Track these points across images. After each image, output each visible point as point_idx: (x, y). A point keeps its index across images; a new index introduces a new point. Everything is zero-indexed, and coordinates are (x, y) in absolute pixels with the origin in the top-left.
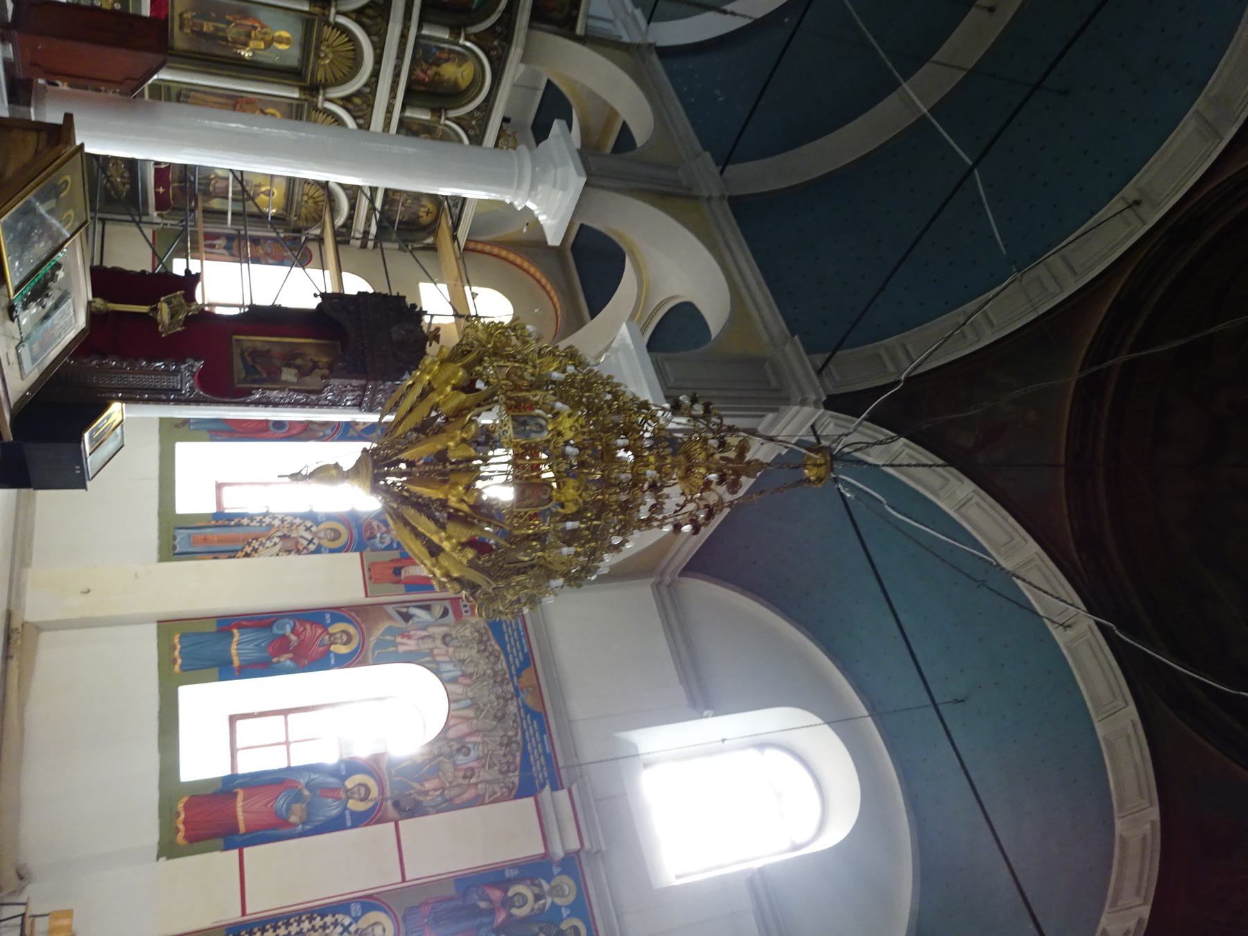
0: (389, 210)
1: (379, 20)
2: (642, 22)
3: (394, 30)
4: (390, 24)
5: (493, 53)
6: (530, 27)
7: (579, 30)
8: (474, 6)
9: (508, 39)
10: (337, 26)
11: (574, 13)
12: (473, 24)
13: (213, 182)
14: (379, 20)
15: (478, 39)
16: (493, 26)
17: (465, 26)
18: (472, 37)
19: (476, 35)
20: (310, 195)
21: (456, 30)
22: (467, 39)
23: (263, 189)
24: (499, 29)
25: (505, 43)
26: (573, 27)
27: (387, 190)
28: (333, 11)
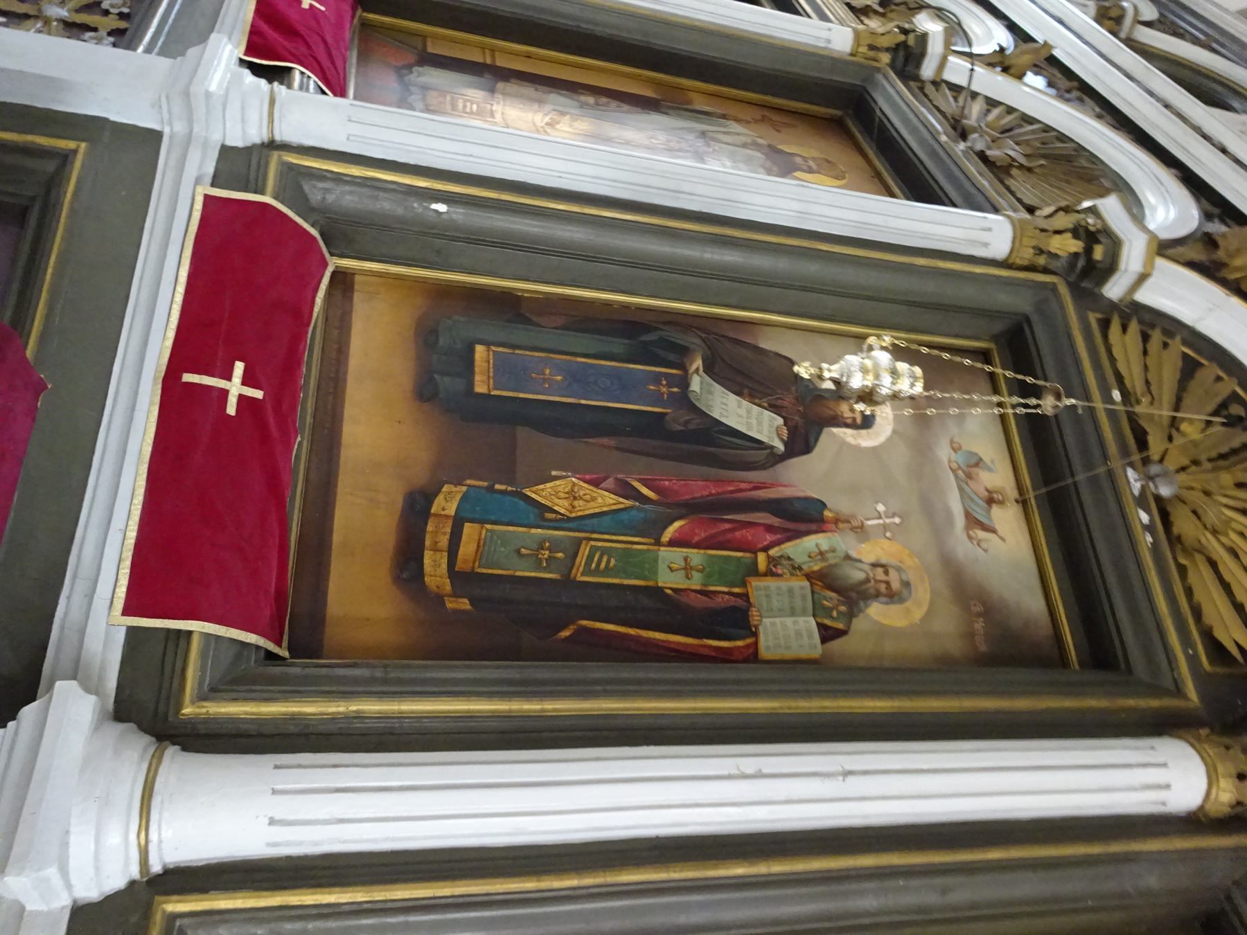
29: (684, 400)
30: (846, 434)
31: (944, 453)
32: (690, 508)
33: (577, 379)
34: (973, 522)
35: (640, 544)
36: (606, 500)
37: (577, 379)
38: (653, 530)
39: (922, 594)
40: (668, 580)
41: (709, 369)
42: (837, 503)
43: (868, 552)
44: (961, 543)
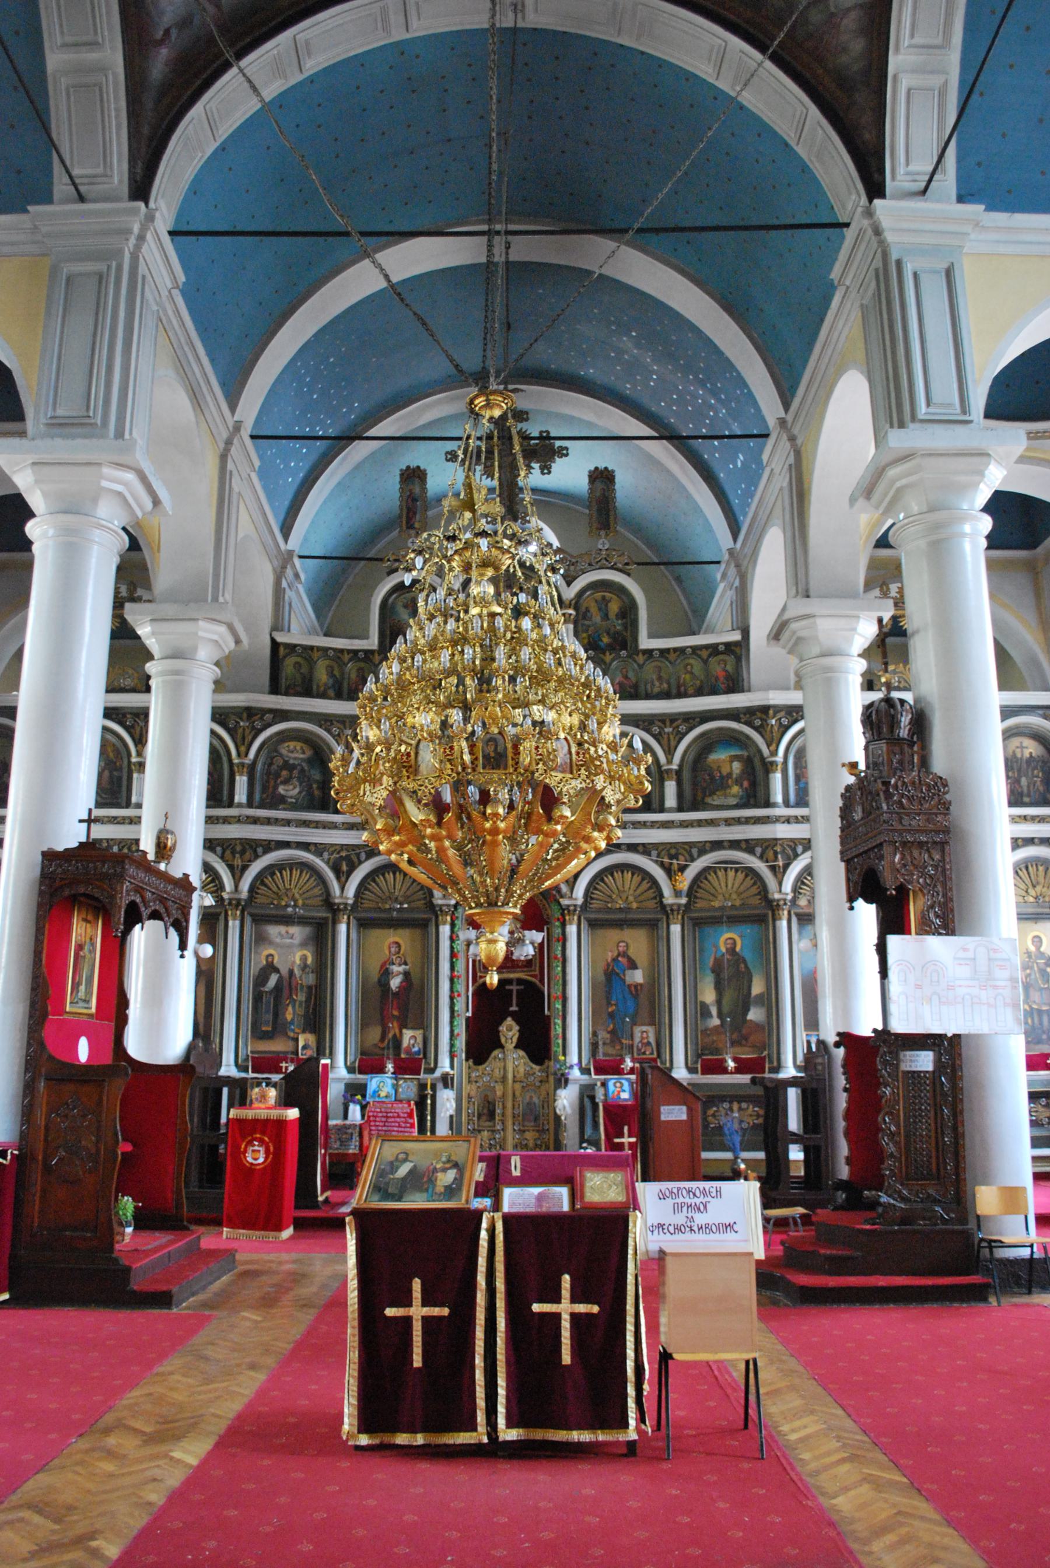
0: (1029, 795)
1: (778, 849)
2: (723, 566)
3: (782, 831)
4: (779, 836)
5: (785, 721)
6: (749, 691)
7: (736, 636)
8: (746, 754)
9: (765, 710)
10: (796, 890)
11: (721, 648)
12: (760, 751)
13: (1035, 1006)
14: (778, 849)
15: (773, 742)
16: (756, 729)
17: (763, 759)
18: (773, 748)
19: (768, 746)
20: (1024, 894)
21: (768, 767)
22: (775, 753)
23: (1032, 948)
24: (758, 722)
25: (771, 712)
26: (736, 644)
27: (1012, 804)
28: (777, 896)
29: (271, 992)
30: (275, 962)
31: (278, 940)
32: (291, 995)
33: (267, 1012)
34: (292, 938)
35: (297, 1004)
36: (290, 1008)
37: (267, 1012)
38: (295, 1001)
39: (305, 952)
40: (304, 999)
41: (264, 986)
42: (289, 966)
43: (298, 962)
44: (297, 941)
